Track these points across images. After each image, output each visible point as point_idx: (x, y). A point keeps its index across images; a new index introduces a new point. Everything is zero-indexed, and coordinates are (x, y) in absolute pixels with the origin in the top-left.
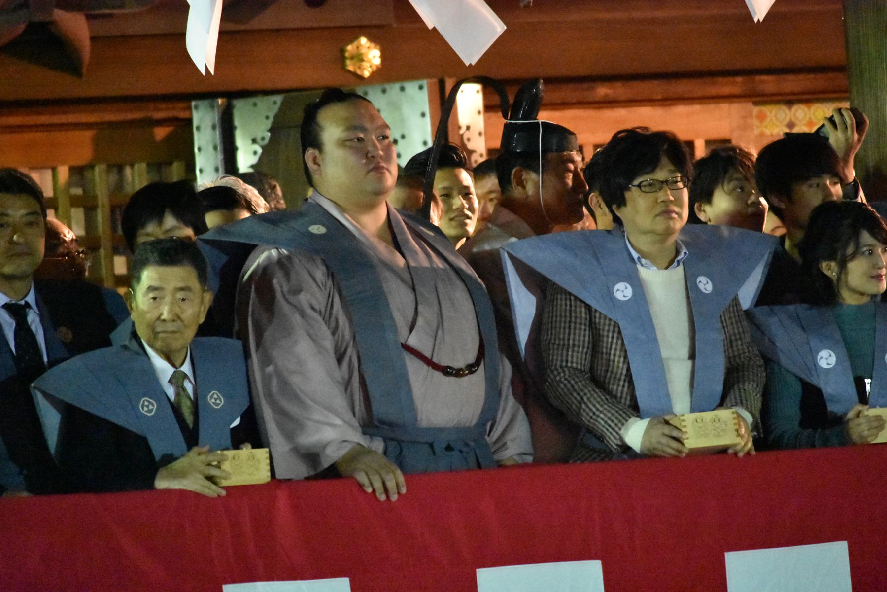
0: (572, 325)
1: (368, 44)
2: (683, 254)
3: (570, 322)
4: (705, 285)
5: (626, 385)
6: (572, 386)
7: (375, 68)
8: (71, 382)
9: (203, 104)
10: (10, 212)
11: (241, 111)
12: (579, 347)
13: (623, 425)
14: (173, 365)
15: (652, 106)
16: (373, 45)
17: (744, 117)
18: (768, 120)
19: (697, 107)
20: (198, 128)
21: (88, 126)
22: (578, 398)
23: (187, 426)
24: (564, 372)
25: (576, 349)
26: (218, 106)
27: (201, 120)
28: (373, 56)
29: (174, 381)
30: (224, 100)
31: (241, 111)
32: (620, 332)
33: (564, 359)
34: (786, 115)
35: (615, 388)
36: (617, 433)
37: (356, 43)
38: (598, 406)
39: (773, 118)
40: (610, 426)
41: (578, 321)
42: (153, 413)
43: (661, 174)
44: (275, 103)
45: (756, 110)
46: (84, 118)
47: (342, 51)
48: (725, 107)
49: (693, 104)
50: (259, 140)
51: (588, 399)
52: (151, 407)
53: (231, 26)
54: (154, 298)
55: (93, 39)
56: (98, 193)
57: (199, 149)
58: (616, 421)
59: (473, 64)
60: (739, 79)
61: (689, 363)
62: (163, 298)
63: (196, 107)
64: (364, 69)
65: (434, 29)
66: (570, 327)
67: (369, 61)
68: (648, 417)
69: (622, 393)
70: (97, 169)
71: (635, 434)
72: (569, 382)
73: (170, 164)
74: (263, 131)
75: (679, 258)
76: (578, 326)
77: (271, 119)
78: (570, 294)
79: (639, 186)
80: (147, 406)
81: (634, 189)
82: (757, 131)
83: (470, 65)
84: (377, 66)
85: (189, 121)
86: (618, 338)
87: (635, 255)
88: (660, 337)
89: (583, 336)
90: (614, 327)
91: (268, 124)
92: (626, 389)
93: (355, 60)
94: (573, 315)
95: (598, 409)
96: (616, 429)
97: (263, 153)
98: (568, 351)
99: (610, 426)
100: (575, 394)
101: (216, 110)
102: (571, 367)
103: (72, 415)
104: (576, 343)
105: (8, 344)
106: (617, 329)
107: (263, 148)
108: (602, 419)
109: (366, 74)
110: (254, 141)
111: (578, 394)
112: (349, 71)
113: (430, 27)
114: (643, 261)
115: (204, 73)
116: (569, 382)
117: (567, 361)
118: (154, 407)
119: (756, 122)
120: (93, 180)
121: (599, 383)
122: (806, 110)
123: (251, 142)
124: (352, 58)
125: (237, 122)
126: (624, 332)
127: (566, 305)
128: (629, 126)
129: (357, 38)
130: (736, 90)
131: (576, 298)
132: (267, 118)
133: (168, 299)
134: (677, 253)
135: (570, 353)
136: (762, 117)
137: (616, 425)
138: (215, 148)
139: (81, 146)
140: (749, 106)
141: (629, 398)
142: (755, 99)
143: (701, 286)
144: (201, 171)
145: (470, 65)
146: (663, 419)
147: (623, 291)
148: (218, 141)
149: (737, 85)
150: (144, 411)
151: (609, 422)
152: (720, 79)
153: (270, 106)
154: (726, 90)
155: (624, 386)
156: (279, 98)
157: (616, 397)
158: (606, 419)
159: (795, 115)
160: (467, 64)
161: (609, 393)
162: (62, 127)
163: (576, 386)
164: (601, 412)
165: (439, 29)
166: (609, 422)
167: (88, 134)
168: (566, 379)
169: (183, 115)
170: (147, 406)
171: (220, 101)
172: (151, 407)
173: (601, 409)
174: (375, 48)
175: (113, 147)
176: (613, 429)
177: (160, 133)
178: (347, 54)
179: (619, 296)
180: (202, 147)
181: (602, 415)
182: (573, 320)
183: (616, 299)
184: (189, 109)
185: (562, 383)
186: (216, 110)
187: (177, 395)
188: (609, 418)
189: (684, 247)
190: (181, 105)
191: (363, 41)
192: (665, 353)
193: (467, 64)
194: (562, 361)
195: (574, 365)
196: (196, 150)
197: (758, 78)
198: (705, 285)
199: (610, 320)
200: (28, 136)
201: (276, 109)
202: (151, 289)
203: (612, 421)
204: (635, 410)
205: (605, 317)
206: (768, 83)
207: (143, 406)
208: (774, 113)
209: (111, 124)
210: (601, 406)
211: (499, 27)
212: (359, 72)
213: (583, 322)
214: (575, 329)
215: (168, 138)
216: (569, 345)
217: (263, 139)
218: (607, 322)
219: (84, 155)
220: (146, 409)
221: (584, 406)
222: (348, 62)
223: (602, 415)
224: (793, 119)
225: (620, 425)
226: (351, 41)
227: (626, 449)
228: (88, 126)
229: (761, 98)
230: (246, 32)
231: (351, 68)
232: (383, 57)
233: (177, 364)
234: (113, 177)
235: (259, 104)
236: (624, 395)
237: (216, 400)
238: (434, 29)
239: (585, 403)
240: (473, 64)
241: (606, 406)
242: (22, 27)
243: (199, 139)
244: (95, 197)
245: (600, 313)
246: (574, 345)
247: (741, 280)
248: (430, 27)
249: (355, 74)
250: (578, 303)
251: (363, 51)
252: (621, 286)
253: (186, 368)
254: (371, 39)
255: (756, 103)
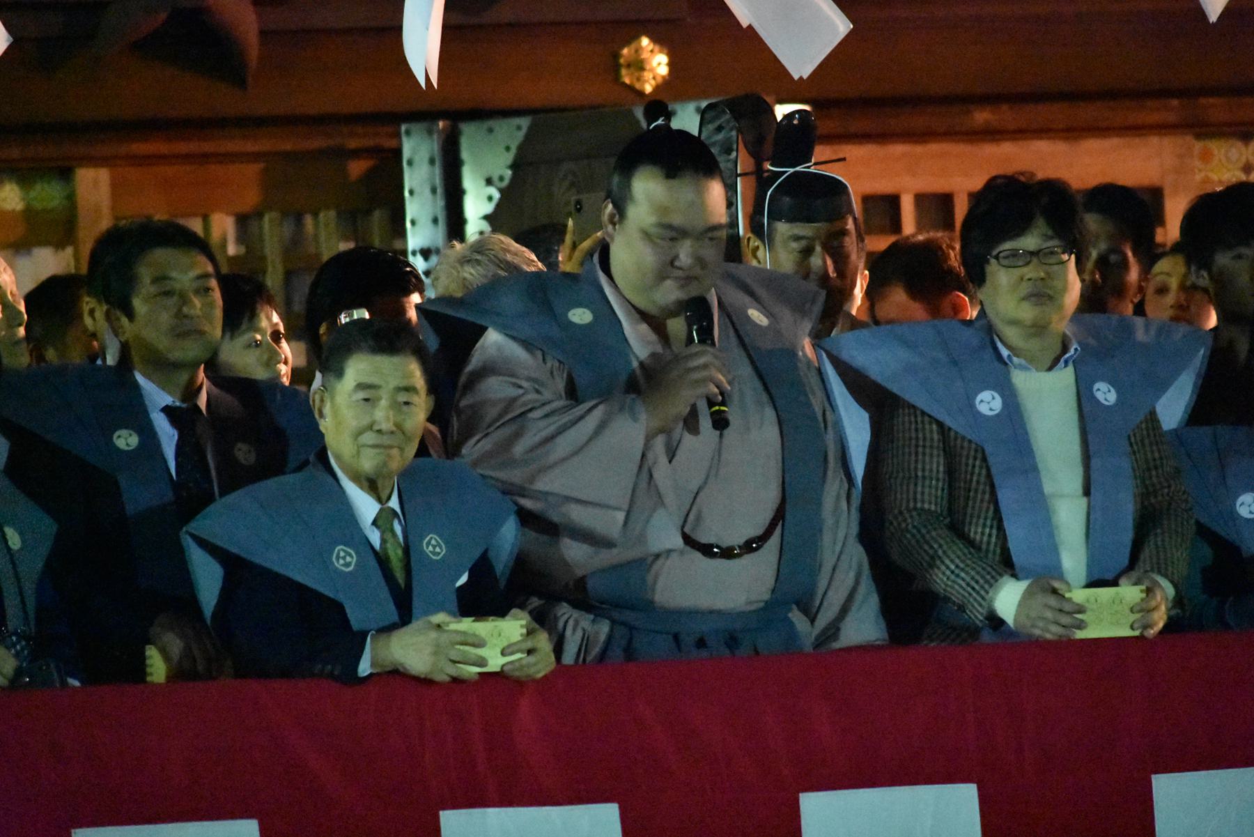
0: (920, 449)
1: (651, 46)
2: (1072, 351)
3: (917, 446)
4: (1105, 394)
5: (994, 532)
6: (923, 536)
7: (659, 80)
8: (240, 521)
9: (417, 128)
10: (174, 274)
11: (471, 139)
12: (931, 479)
13: (991, 586)
14: (379, 500)
15: (1049, 138)
16: (657, 48)
17: (1180, 156)
18: (1215, 161)
19: (1115, 141)
20: (410, 163)
21: (255, 157)
22: (931, 552)
23: (398, 585)
24: (911, 517)
25: (927, 482)
26: (439, 131)
27: (414, 151)
28: (659, 64)
29: (379, 523)
30: (448, 122)
31: (471, 139)
32: (984, 459)
33: (911, 496)
34: (1241, 154)
35: (978, 538)
36: (983, 598)
37: (633, 46)
38: (957, 561)
39: (1224, 160)
40: (973, 589)
41: (928, 444)
42: (351, 568)
43: (1030, 242)
44: (519, 128)
45: (1198, 146)
46: (251, 147)
47: (616, 56)
48: (1154, 140)
49: (1109, 136)
50: (495, 179)
51: (944, 552)
52: (348, 559)
53: (458, 19)
54: (366, 400)
55: (263, 33)
56: (267, 251)
57: (411, 192)
58: (982, 581)
59: (805, 77)
60: (1175, 102)
61: (1084, 501)
62: (379, 399)
63: (408, 133)
64: (646, 81)
65: (750, 27)
66: (917, 454)
67: (652, 70)
68: (1027, 578)
69: (989, 543)
70: (266, 218)
71: (1008, 599)
72: (919, 531)
73: (369, 212)
74: (501, 165)
75: (1067, 356)
76: (928, 451)
77: (513, 151)
78: (914, 407)
79: (997, 257)
80: (344, 558)
81: (993, 261)
82: (1198, 177)
83: (801, 78)
84: (663, 77)
85: (398, 153)
86: (981, 467)
87: (1005, 352)
88: (1040, 466)
89: (936, 464)
90: (976, 451)
91: (509, 158)
92: (993, 539)
93: (632, 69)
94: (920, 435)
95: (957, 566)
96: (983, 593)
97: (501, 199)
98: (916, 485)
99: (973, 589)
100: (926, 547)
101: (435, 136)
102: (922, 509)
103: (235, 567)
104: (927, 474)
105: (165, 462)
106: (979, 455)
107: (501, 191)
108: (963, 580)
109: (648, 89)
110: (489, 182)
111: (931, 547)
112: (624, 83)
113: (745, 24)
114: (1015, 359)
115: (423, 85)
116: (919, 531)
117: (915, 500)
118: (353, 560)
119: (1198, 163)
120: (261, 235)
121: (958, 530)
122: (1243, 149)
123: (483, 183)
124: (629, 66)
125: (465, 155)
126: (991, 460)
127: (910, 423)
128: (1009, 170)
129: (637, 37)
130: (1172, 118)
131: (923, 413)
132: (508, 149)
133: (384, 403)
134: (1065, 349)
135: (919, 489)
136: (1206, 157)
137: (982, 587)
138: (434, 191)
139: (246, 183)
140: (1189, 139)
141: (998, 551)
142: (1198, 130)
143: (1100, 396)
144: (413, 223)
145: (801, 78)
146: (1047, 582)
147: (989, 403)
148: (438, 181)
149: (1172, 110)
150: (339, 564)
151: (973, 583)
152: (1149, 103)
153: (512, 132)
154: (1155, 118)
155: (990, 535)
156: (525, 122)
157: (979, 549)
158: (968, 579)
159: (1241, 154)
160: (796, 77)
161: (971, 543)
162: (205, 158)
163: (928, 536)
164: (962, 570)
165: (756, 26)
166: (973, 583)
167: (253, 170)
168: (914, 527)
169: (390, 143)
170: (344, 558)
171: (441, 124)
172: (348, 559)
173: (962, 565)
174: (661, 52)
175: (288, 188)
176: (978, 593)
177: (357, 168)
178: (622, 61)
179: (984, 409)
180: (417, 190)
181: (963, 575)
182: (921, 443)
183: (979, 413)
184: (398, 135)
185: (908, 531)
186: (435, 136)
187: (383, 541)
188: (973, 578)
189: (1074, 341)
190: (390, 129)
191: (645, 41)
192: (1048, 488)
193: (796, 77)
194: (908, 501)
195: (926, 506)
196: (407, 194)
197: (1203, 101)
198: (1105, 394)
199: (970, 441)
200: (169, 171)
201: (520, 135)
202: (361, 386)
203: (977, 582)
204: (1008, 566)
205: (963, 438)
206: (1216, 109)
207: (338, 557)
208: (1223, 151)
209: (286, 155)
210: (963, 561)
211: (841, 26)
212: (637, 86)
213: (936, 444)
214: (924, 454)
215: (369, 176)
216: (917, 476)
217: (501, 179)
218: (966, 444)
219: (251, 198)
220: (341, 562)
221: (938, 562)
222: (624, 72)
223: (963, 575)
224: (1241, 165)
225: (986, 586)
226: (627, 42)
227: (995, 622)
228: (255, 157)
229: (1203, 129)
230: (481, 26)
231: (627, 81)
232: (671, 64)
233: (384, 497)
234: (287, 229)
235: (497, 128)
236: (992, 547)
237: (434, 547)
238: (750, 27)
239: (940, 558)
240: (805, 77)
241: (969, 562)
242: (163, 16)
243: (410, 177)
244: (263, 258)
245: (956, 433)
246: (924, 477)
247: (1162, 386)
248: (745, 24)
249: (631, 88)
250: (926, 419)
251: (645, 55)
252: (986, 395)
253: (394, 503)
254: (655, 39)
255: (1199, 136)
